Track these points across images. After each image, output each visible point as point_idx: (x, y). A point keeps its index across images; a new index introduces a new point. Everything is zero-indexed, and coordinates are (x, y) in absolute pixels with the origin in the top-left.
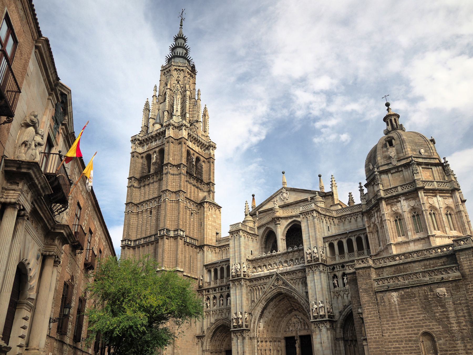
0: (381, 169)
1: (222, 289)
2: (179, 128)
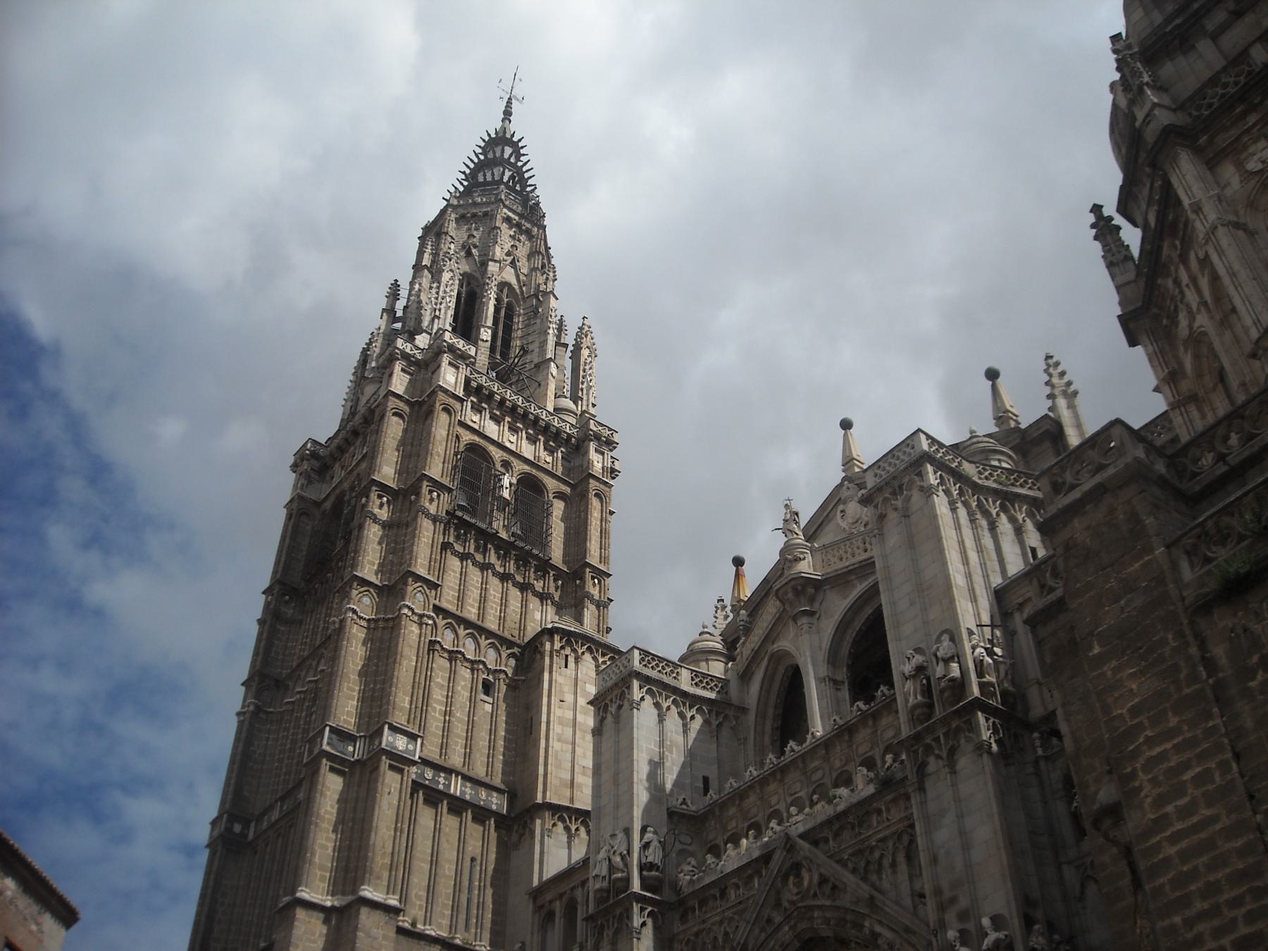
2: (431, 368)
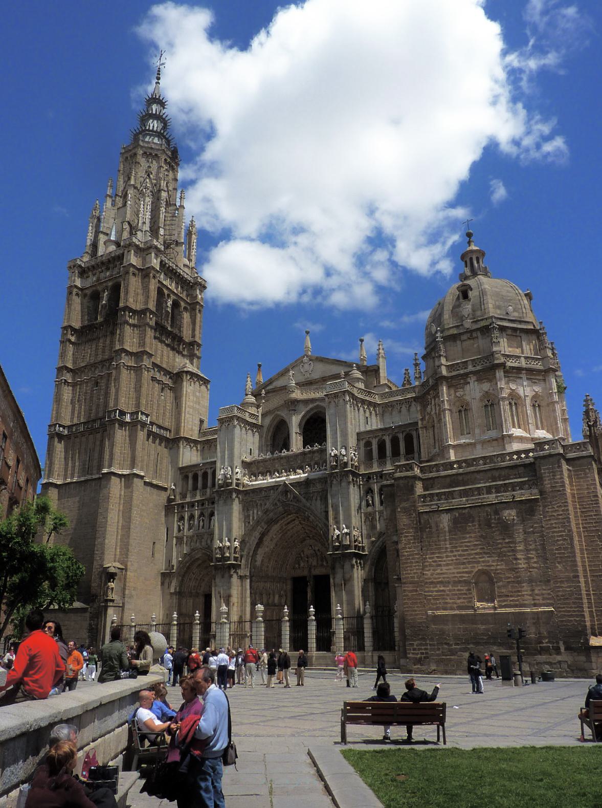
0: (447, 333)
1: (203, 505)
2: (145, 253)
